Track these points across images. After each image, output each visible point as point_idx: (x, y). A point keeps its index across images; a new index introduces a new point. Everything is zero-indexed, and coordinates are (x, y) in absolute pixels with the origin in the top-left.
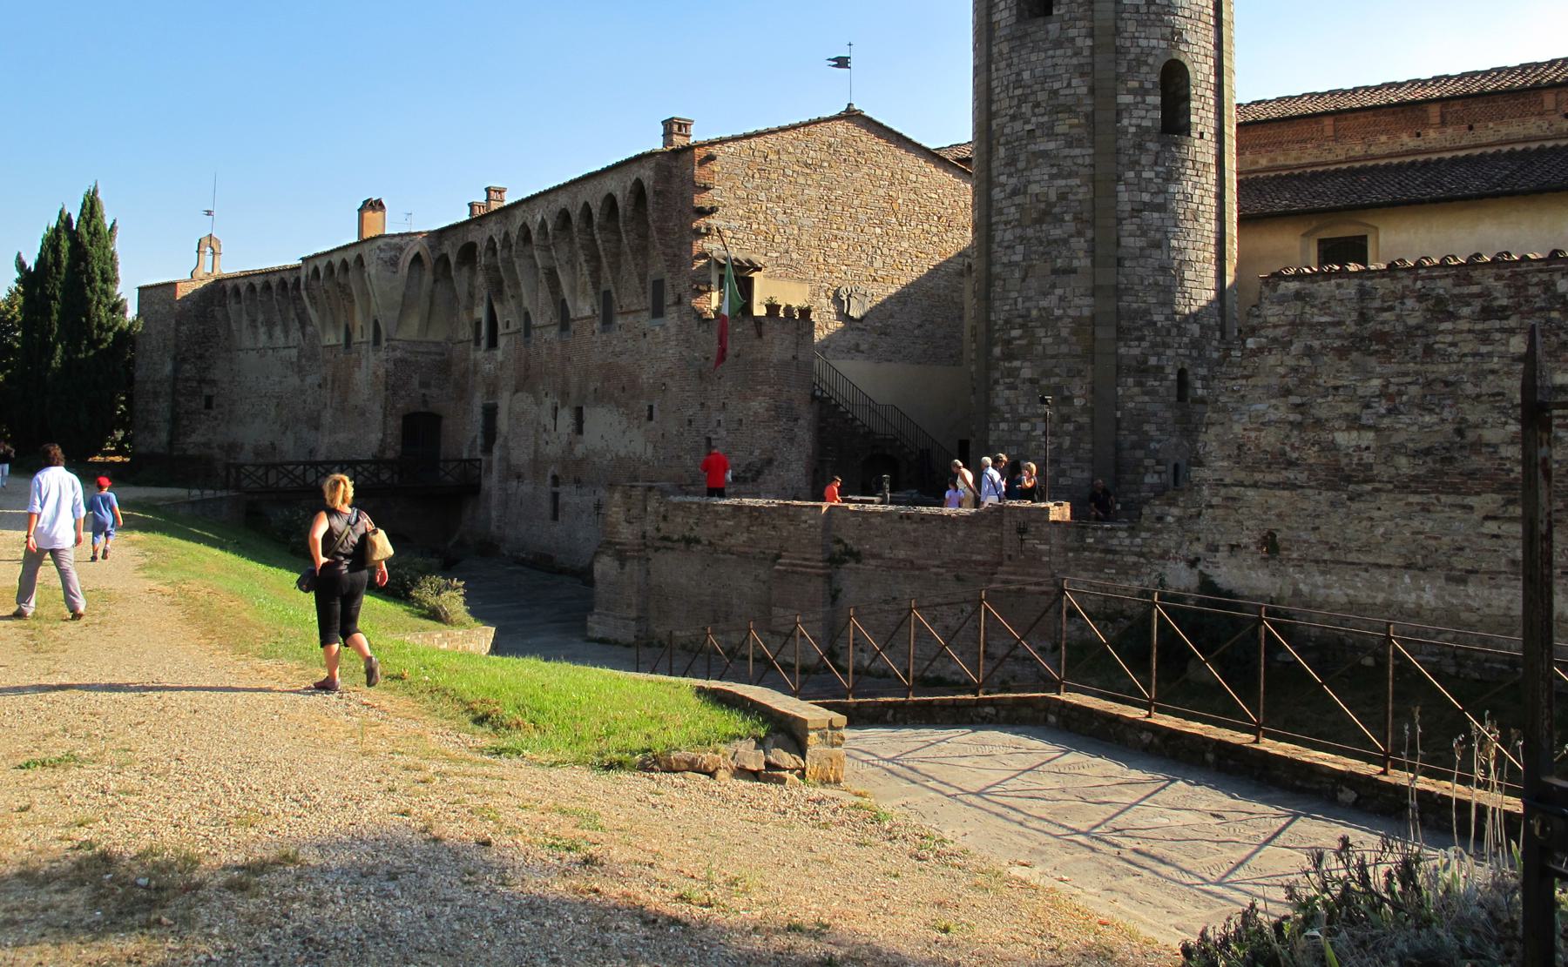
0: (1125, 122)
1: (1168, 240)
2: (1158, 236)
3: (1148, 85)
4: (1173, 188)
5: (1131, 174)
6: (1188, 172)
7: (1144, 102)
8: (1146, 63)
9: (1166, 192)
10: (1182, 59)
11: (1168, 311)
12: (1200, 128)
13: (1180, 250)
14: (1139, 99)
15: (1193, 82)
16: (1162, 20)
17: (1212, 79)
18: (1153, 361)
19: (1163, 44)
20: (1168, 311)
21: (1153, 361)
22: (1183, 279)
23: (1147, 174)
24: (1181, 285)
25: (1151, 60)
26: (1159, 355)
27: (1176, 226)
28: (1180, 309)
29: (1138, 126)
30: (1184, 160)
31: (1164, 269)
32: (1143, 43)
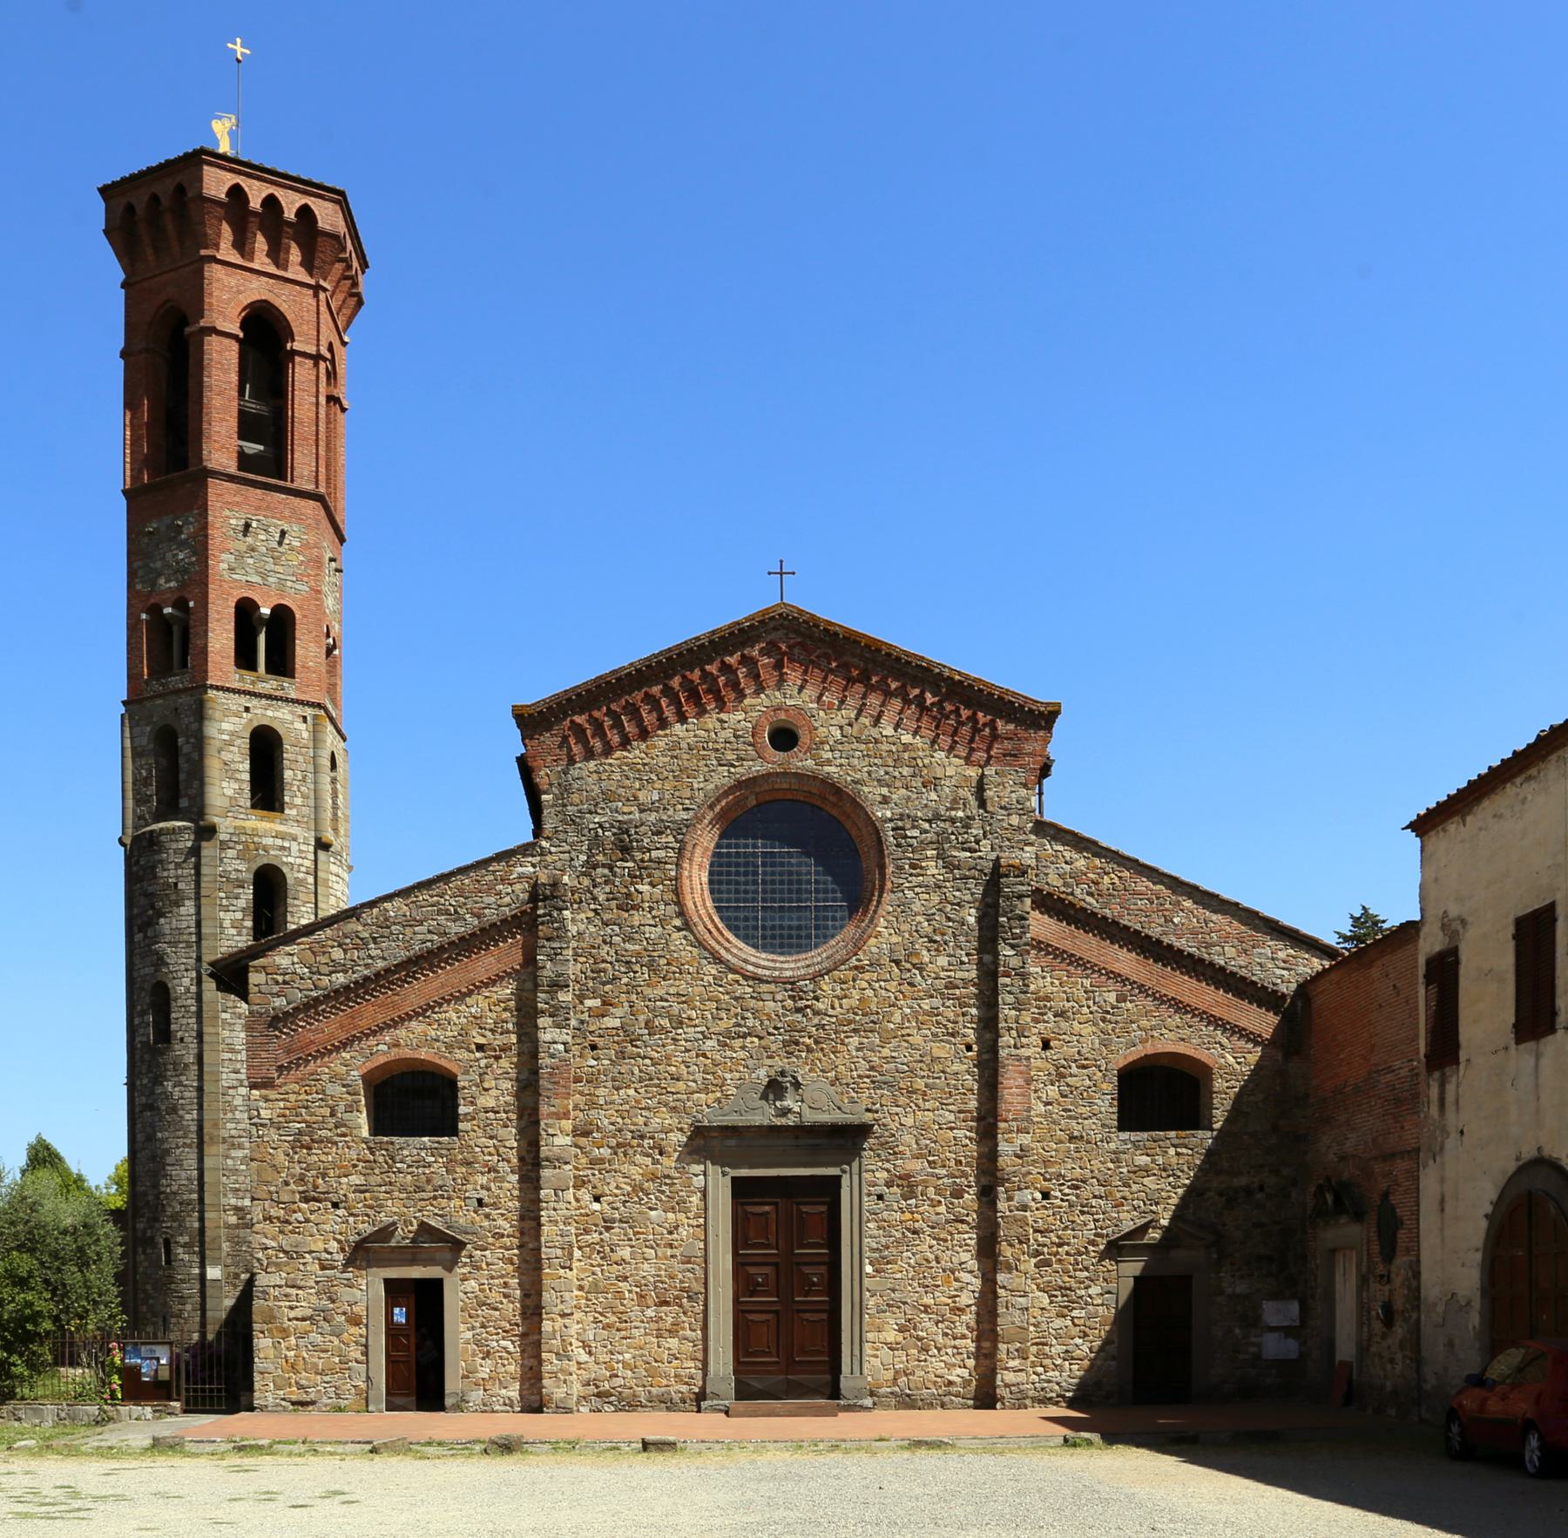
4: (159, 1090)
6: (169, 1073)
12: (179, 1034)
13: (163, 1141)
15: (173, 995)
16: (150, 950)
17: (193, 989)
23: (145, 1081)
24: (164, 1169)
27: (160, 1121)
28: (163, 1189)
29: (141, 1042)
30: (165, 1065)
31: (153, 1158)
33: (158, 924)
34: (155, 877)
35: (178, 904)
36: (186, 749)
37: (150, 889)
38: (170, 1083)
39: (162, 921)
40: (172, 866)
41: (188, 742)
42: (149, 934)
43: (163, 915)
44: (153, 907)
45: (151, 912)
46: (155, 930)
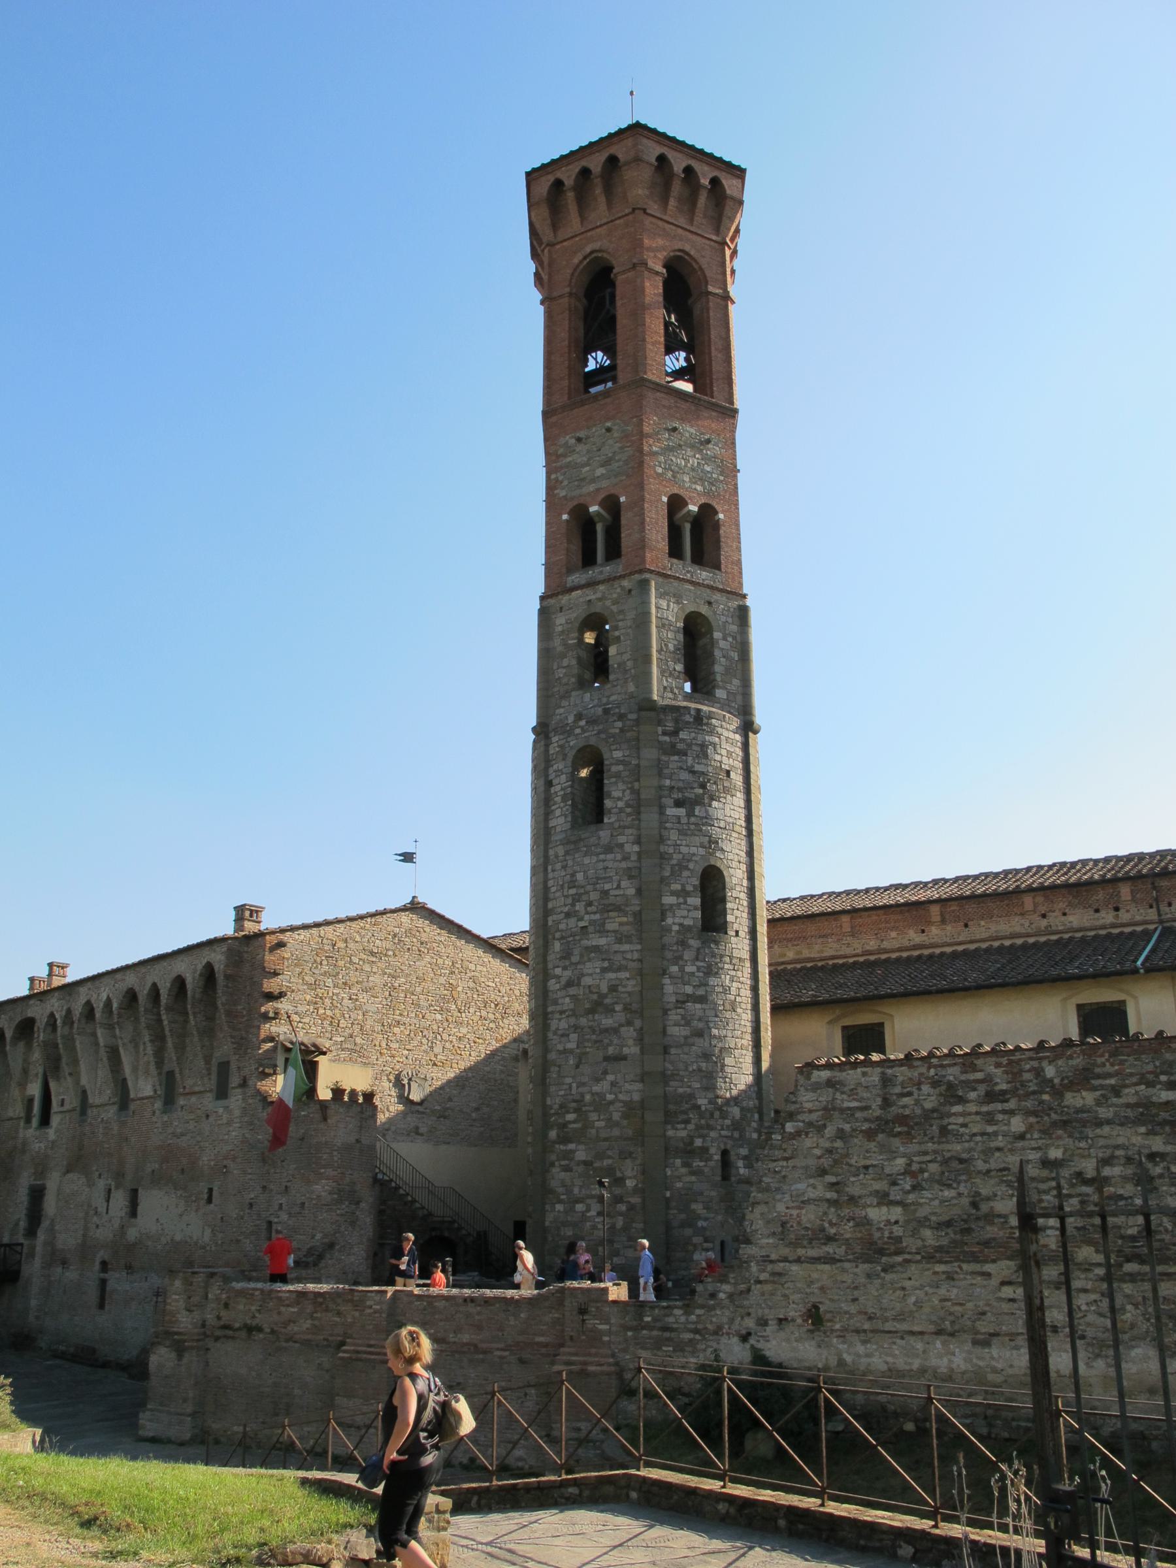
0: (669, 921)
1: (710, 1028)
2: (701, 1025)
3: (689, 888)
4: (713, 981)
5: (674, 969)
6: (726, 966)
7: (685, 903)
8: (687, 868)
9: (706, 985)
10: (718, 865)
11: (710, 1095)
12: (736, 926)
13: (720, 1038)
14: (681, 900)
15: (728, 885)
16: (701, 830)
17: (745, 883)
18: (698, 1142)
19: (702, 851)
20: (710, 1095)
21: (698, 1142)
22: (723, 1065)
23: (689, 969)
24: (722, 1070)
25: (691, 866)
26: (703, 1137)
27: (716, 1016)
28: (721, 1093)
29: (681, 925)
30: (722, 956)
31: (707, 1056)
32: (684, 850)
33: (710, 806)
34: (706, 756)
35: (727, 790)
36: (722, 644)
37: (698, 768)
38: (728, 977)
39: (715, 804)
40: (724, 752)
41: (725, 639)
42: (697, 813)
43: (712, 798)
44: (703, 786)
45: (701, 791)
46: (707, 811)
